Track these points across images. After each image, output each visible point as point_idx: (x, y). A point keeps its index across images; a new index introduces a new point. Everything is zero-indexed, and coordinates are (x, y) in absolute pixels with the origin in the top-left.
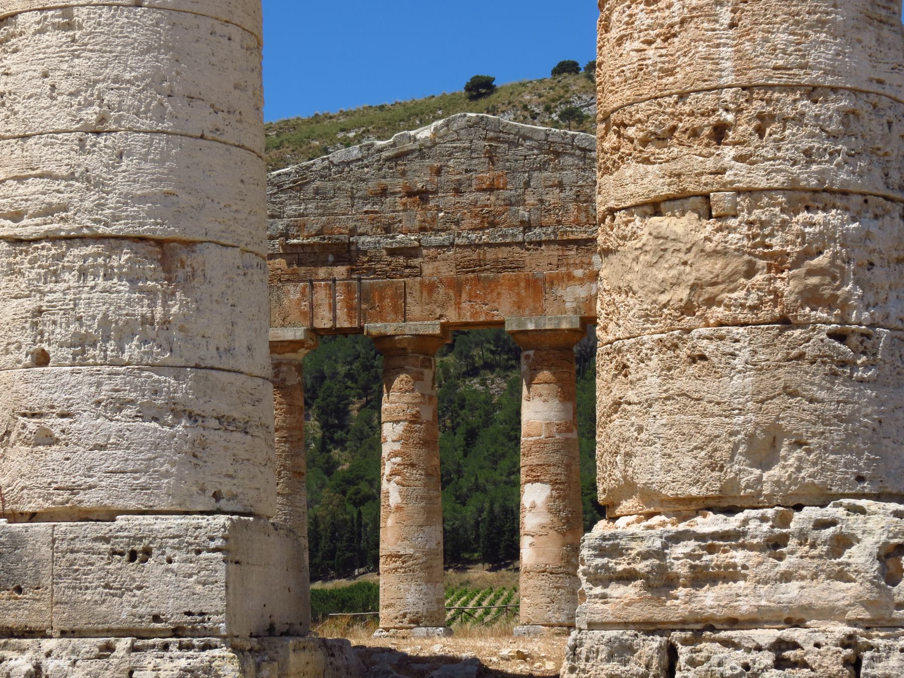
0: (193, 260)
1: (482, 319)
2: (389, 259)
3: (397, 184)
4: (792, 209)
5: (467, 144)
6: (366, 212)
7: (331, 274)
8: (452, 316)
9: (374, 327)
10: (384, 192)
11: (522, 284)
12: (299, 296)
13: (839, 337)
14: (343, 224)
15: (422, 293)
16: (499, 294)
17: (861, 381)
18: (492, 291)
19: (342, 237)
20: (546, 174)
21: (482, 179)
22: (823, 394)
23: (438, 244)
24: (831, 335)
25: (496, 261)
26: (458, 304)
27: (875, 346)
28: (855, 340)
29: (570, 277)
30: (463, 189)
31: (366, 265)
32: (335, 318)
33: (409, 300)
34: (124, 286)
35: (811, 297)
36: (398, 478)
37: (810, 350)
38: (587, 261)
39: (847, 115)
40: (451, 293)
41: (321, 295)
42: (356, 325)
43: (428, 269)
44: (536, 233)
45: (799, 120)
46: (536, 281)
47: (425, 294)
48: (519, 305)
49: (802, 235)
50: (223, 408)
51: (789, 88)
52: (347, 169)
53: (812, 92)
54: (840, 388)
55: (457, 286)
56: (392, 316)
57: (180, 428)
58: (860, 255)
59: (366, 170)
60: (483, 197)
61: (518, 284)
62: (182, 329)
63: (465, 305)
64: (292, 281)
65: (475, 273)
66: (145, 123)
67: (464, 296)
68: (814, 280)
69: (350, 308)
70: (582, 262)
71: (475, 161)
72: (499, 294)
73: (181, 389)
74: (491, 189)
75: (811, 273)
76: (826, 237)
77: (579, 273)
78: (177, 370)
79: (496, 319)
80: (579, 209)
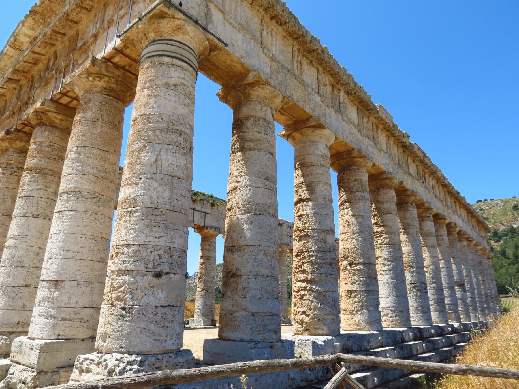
0: (62, 284)
4: (119, 275)
13: (124, 309)
17: (126, 321)
22: (115, 324)
24: (121, 308)
27: (133, 311)
28: (127, 310)
34: (47, 290)
35: (118, 299)
37: (115, 313)
39: (135, 252)
45: (123, 253)
49: (119, 282)
50: (64, 316)
51: (123, 245)
53: (128, 246)
54: (120, 323)
57: (51, 321)
58: (133, 287)
62: (56, 299)
66: (57, 257)
68: (119, 294)
73: (53, 312)
75: (119, 292)
76: (124, 283)
78: (53, 308)
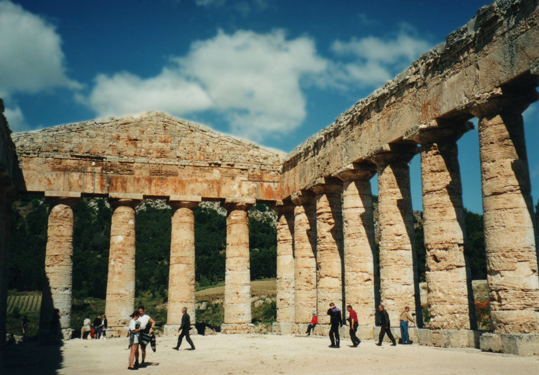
1: (160, 194)
2: (120, 166)
3: (124, 135)
5: (156, 123)
6: (110, 145)
7: (93, 170)
8: (147, 193)
9: (113, 195)
10: (118, 138)
11: (177, 182)
12: (78, 178)
14: (99, 151)
15: (134, 181)
16: (167, 185)
18: (165, 183)
19: (100, 155)
20: (188, 139)
21: (161, 137)
23: (142, 162)
25: (167, 172)
26: (150, 188)
29: (197, 180)
30: (153, 140)
31: (109, 168)
32: (94, 189)
33: (128, 184)
36: (120, 260)
38: (203, 175)
40: (147, 183)
41: (89, 178)
42: (105, 192)
43: (137, 172)
44: (183, 162)
46: (183, 181)
47: (136, 182)
48: (175, 191)
52: (102, 126)
55: (150, 181)
56: (121, 190)
59: (111, 128)
60: (161, 145)
61: (175, 182)
63: (153, 188)
64: (75, 171)
65: (159, 174)
67: (153, 184)
69: (102, 186)
70: (202, 176)
71: (158, 130)
72: (167, 185)
74: (165, 142)
77: (200, 179)
79: (166, 195)
80: (201, 154)
